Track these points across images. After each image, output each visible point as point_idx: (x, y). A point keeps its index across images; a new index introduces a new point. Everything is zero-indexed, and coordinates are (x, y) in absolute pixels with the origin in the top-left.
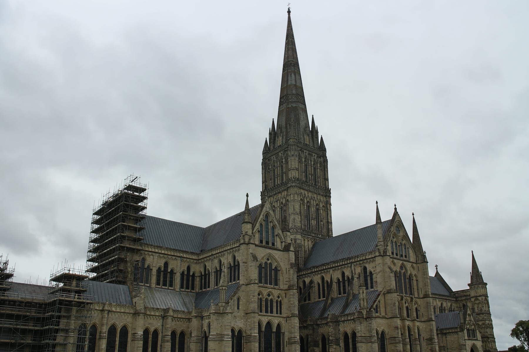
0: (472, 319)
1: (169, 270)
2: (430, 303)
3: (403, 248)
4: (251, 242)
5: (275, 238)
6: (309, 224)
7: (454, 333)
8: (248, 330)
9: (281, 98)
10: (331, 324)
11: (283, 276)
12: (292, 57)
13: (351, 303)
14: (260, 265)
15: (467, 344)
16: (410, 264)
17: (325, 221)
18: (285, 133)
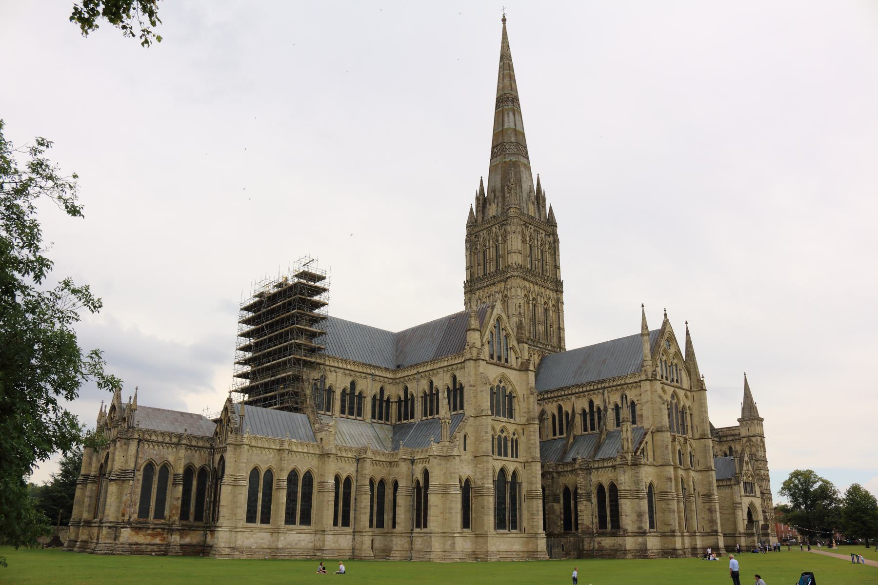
0: (750, 469)
1: (357, 393)
2: (709, 447)
4: (481, 358)
6: (535, 331)
7: (725, 487)
8: (478, 479)
9: (493, 148)
10: (581, 472)
11: (519, 405)
12: (510, 88)
13: (605, 443)
15: (743, 501)
16: (683, 392)
17: (555, 326)
18: (500, 199)
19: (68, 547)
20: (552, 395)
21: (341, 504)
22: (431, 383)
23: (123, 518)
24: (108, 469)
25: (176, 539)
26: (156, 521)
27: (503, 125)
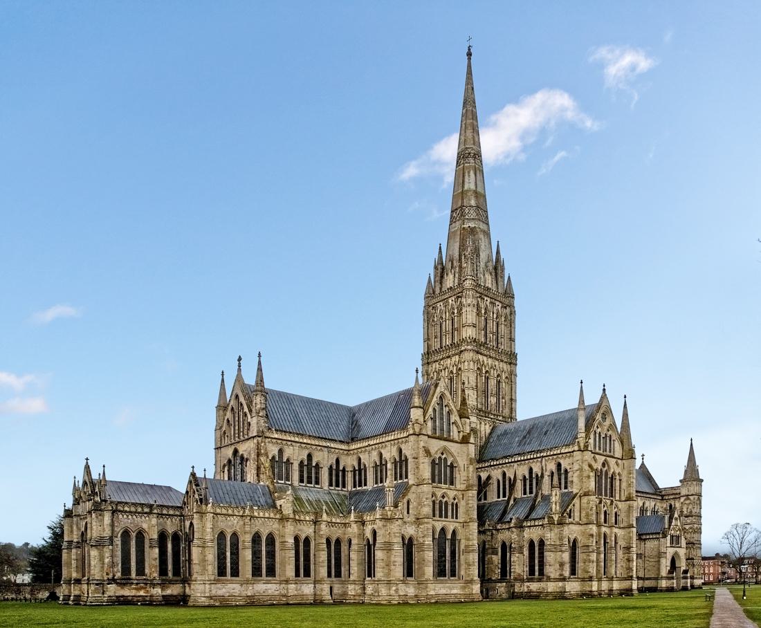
3: (608, 441)
16: (615, 460)
18: (457, 268)
19: (63, 600)
21: (302, 559)
22: (381, 455)
24: (89, 536)
25: (157, 591)
26: (137, 578)
27: (463, 187)
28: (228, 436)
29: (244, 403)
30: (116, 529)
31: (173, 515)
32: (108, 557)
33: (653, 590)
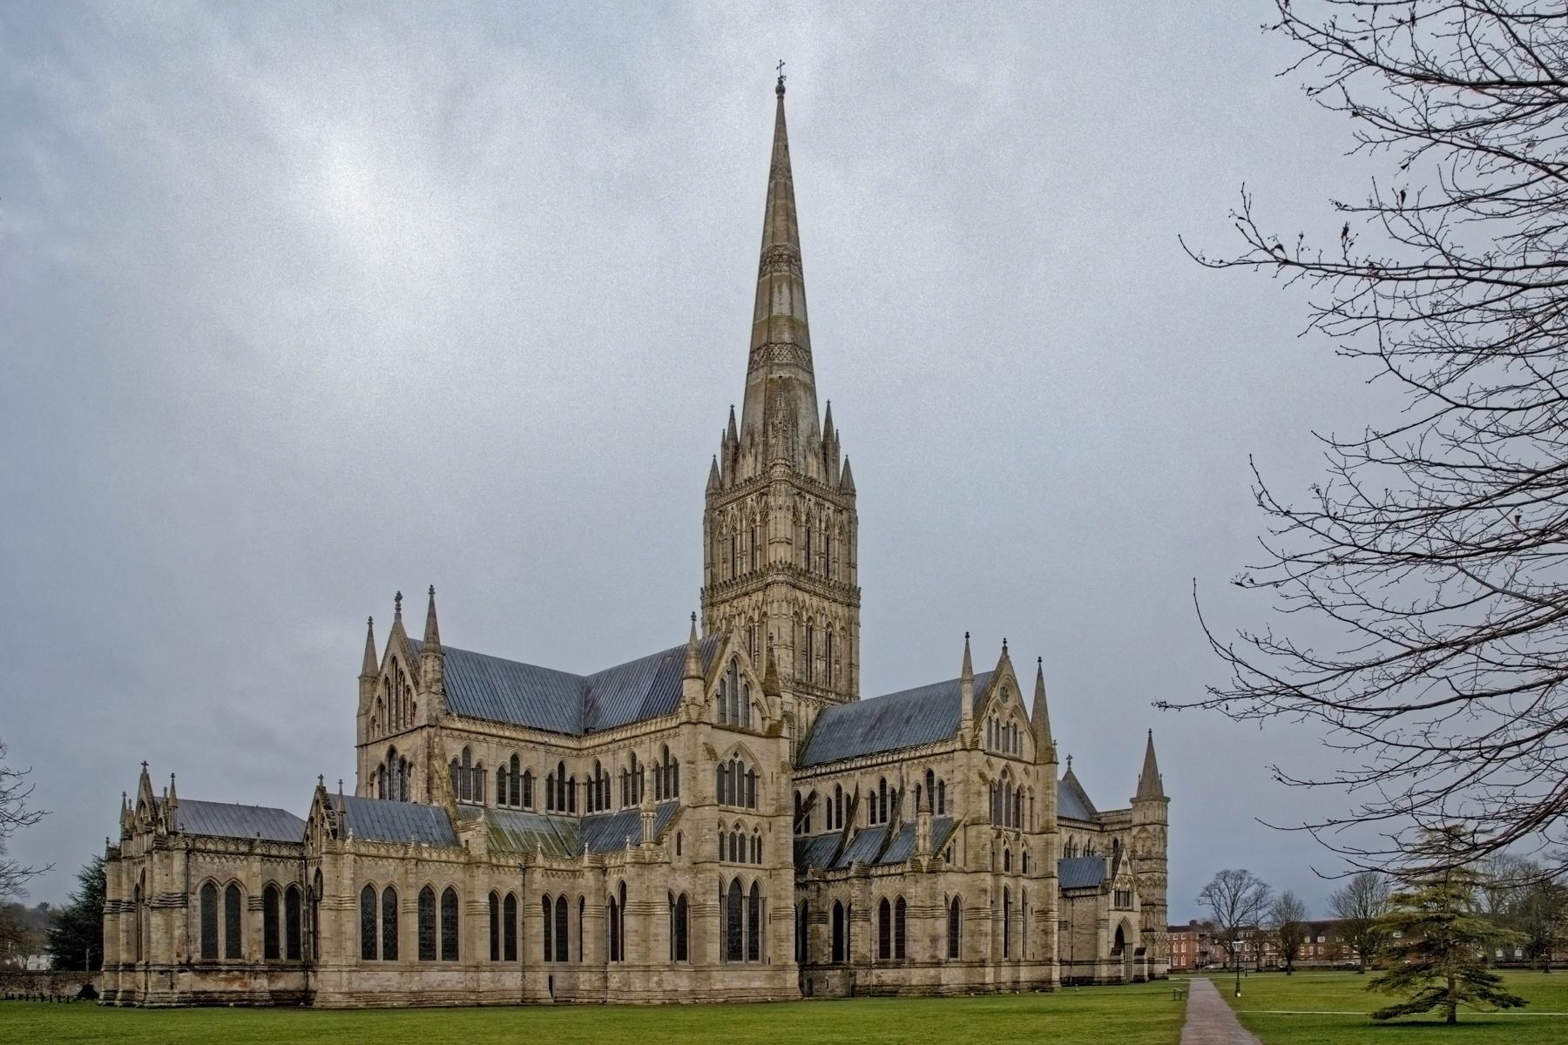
1: (522, 772)
3: (1011, 734)
5: (751, 710)
14: (721, 766)
16: (1022, 766)
18: (761, 447)
19: (105, 999)
20: (828, 770)
22: (633, 757)
23: (179, 959)
24: (147, 893)
25: (262, 984)
26: (229, 961)
27: (770, 311)
28: (379, 726)
29: (406, 670)
30: (192, 880)
31: (288, 858)
32: (179, 928)
33: (1087, 981)
